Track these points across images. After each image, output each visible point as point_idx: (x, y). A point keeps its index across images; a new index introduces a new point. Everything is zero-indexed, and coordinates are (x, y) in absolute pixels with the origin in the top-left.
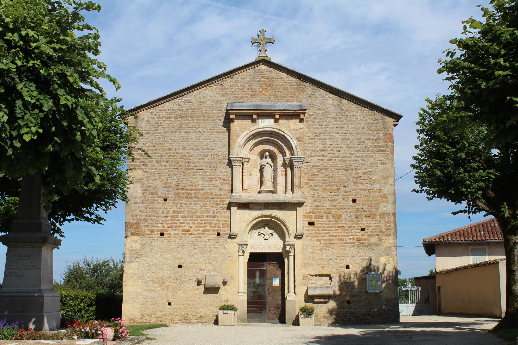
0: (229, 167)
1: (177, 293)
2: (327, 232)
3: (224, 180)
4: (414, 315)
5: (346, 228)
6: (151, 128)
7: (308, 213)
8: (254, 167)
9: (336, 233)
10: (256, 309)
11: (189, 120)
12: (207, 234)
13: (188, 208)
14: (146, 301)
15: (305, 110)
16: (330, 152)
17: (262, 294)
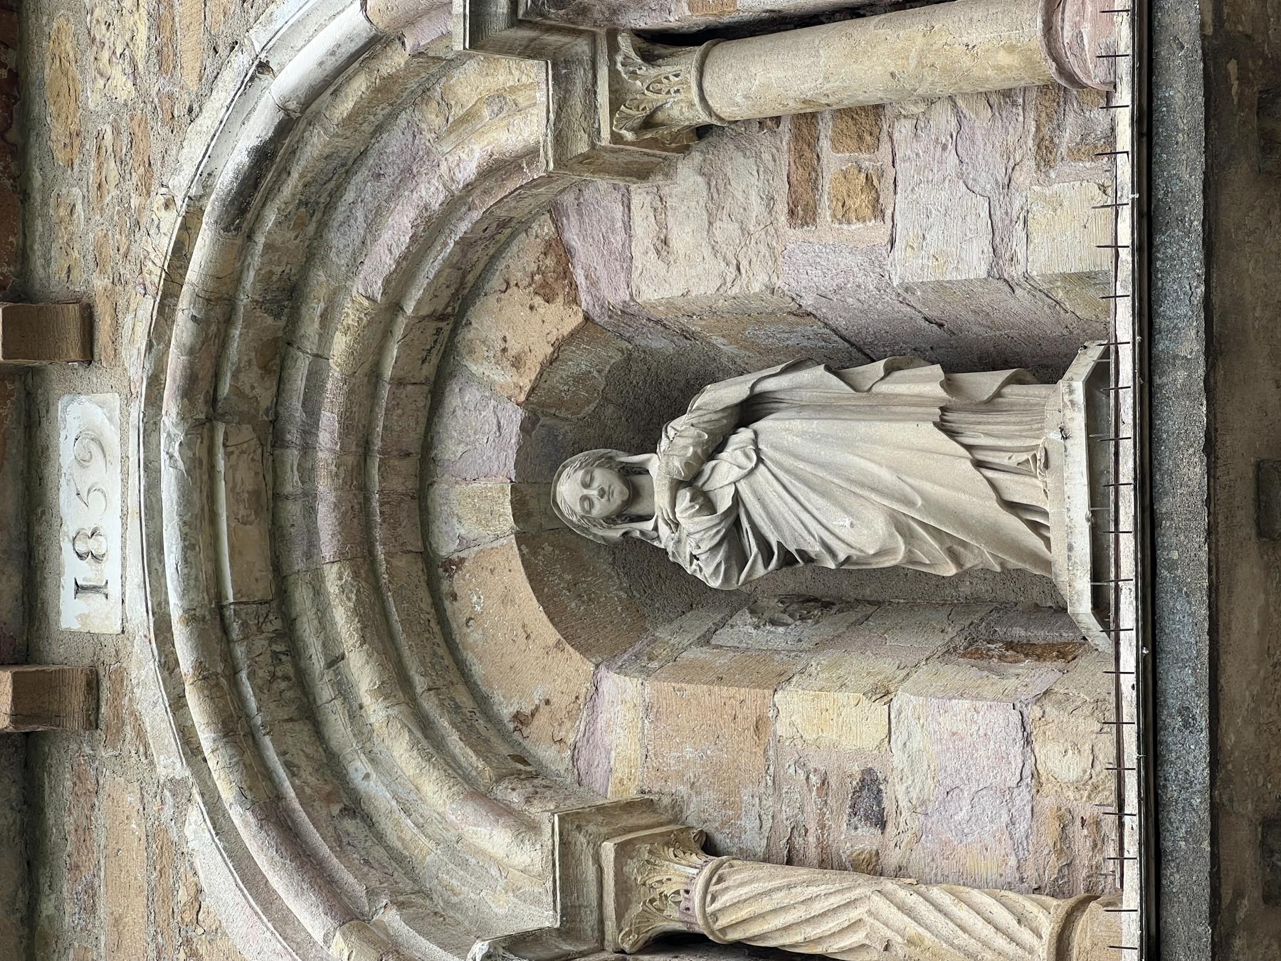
8: (760, 725)
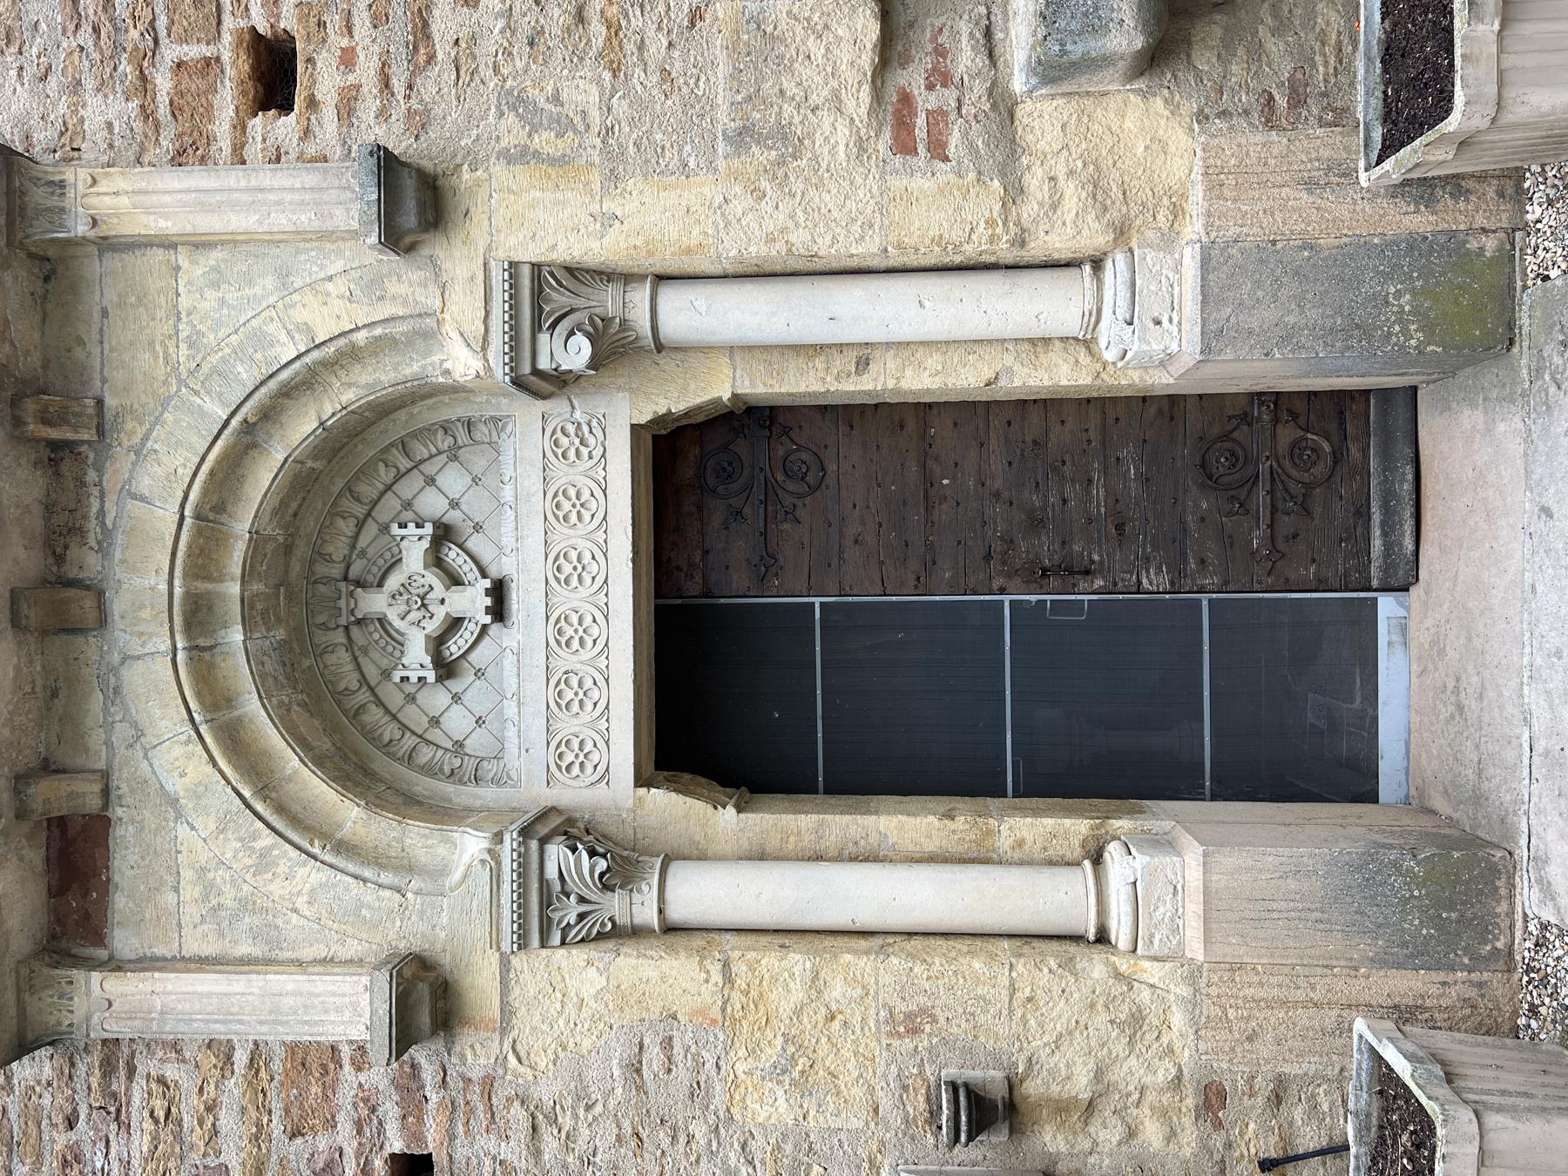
7: (146, 113)
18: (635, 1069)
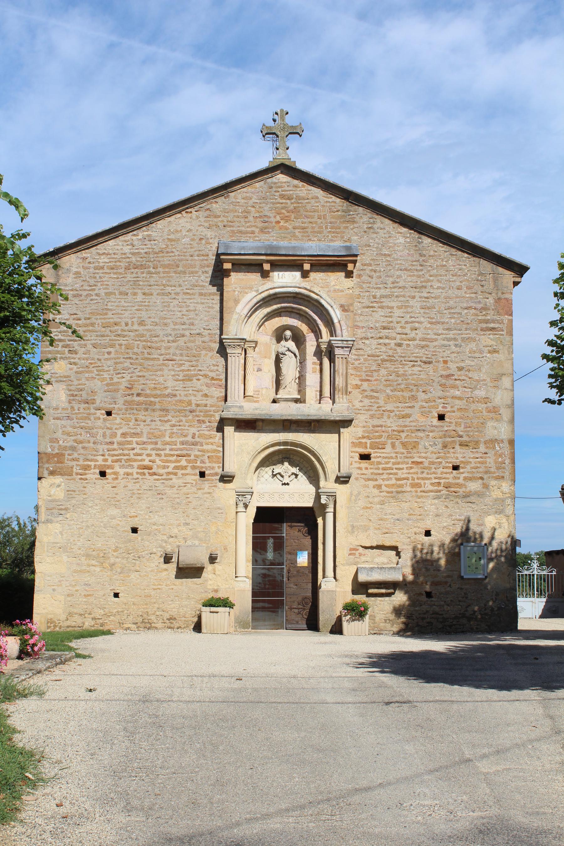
0: (222, 356)
1: (129, 576)
2: (392, 471)
3: (213, 379)
4: (542, 617)
5: (426, 464)
6: (82, 286)
7: (360, 438)
8: (266, 357)
9: (409, 473)
10: (266, 605)
11: (149, 273)
12: (182, 474)
13: (149, 428)
14: (74, 589)
15: (356, 256)
16: (399, 330)
17: (279, 578)
18: (219, 508)
